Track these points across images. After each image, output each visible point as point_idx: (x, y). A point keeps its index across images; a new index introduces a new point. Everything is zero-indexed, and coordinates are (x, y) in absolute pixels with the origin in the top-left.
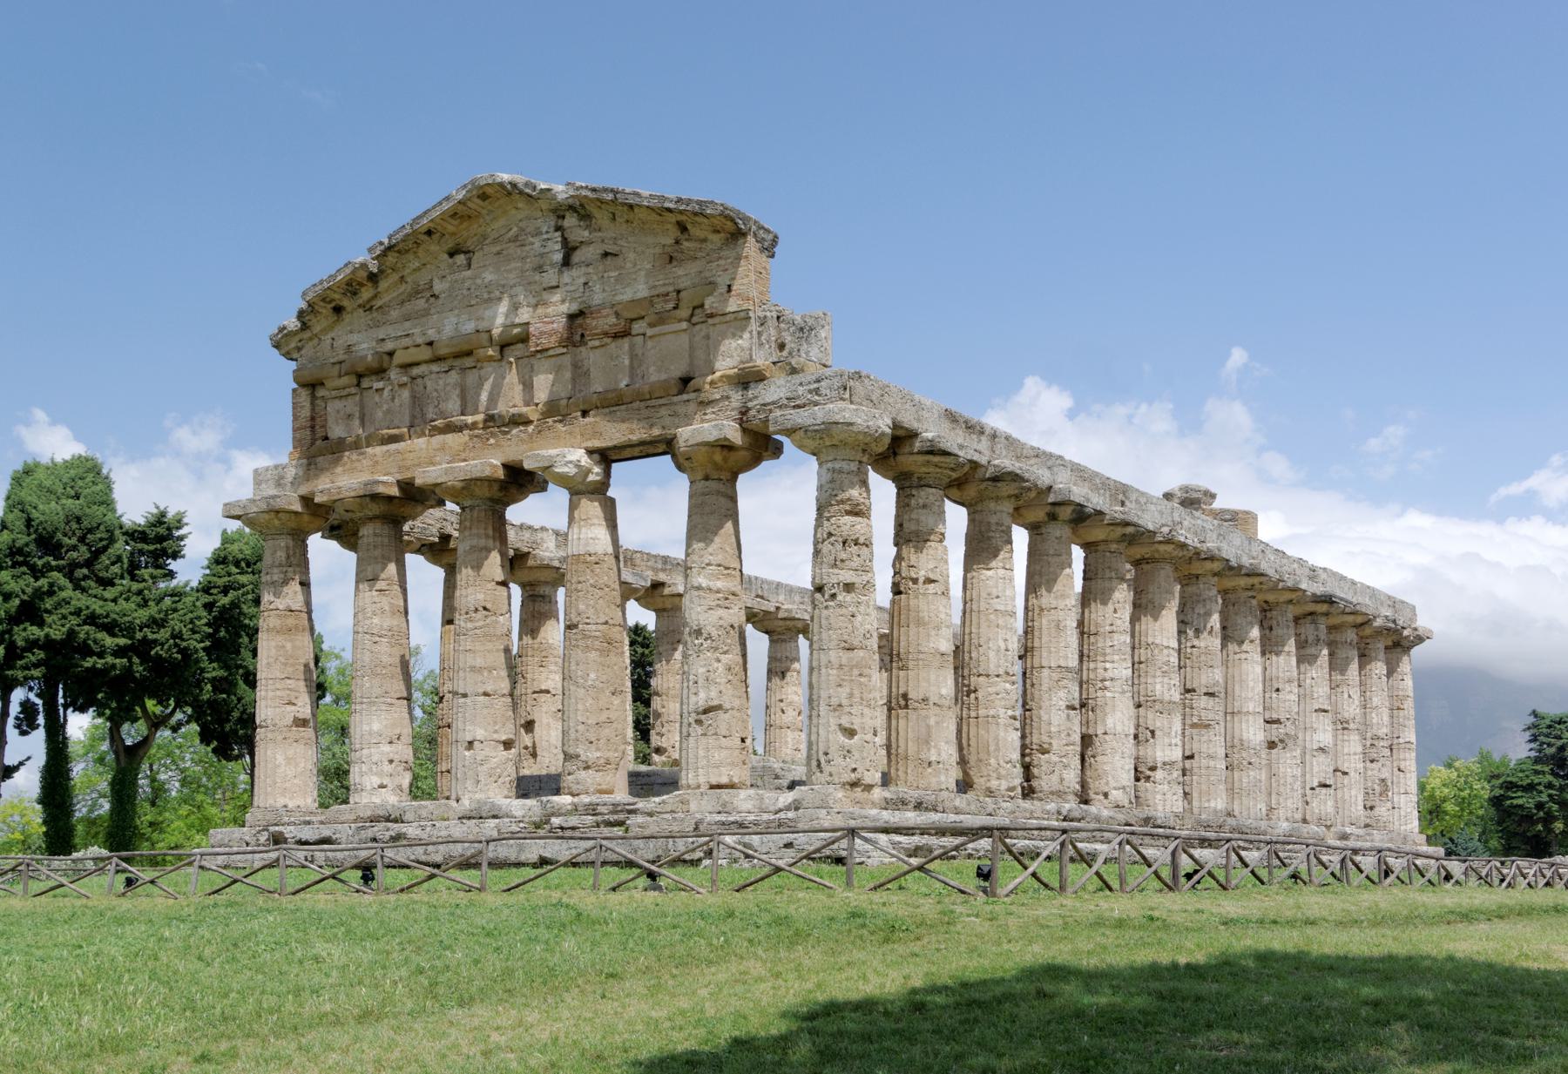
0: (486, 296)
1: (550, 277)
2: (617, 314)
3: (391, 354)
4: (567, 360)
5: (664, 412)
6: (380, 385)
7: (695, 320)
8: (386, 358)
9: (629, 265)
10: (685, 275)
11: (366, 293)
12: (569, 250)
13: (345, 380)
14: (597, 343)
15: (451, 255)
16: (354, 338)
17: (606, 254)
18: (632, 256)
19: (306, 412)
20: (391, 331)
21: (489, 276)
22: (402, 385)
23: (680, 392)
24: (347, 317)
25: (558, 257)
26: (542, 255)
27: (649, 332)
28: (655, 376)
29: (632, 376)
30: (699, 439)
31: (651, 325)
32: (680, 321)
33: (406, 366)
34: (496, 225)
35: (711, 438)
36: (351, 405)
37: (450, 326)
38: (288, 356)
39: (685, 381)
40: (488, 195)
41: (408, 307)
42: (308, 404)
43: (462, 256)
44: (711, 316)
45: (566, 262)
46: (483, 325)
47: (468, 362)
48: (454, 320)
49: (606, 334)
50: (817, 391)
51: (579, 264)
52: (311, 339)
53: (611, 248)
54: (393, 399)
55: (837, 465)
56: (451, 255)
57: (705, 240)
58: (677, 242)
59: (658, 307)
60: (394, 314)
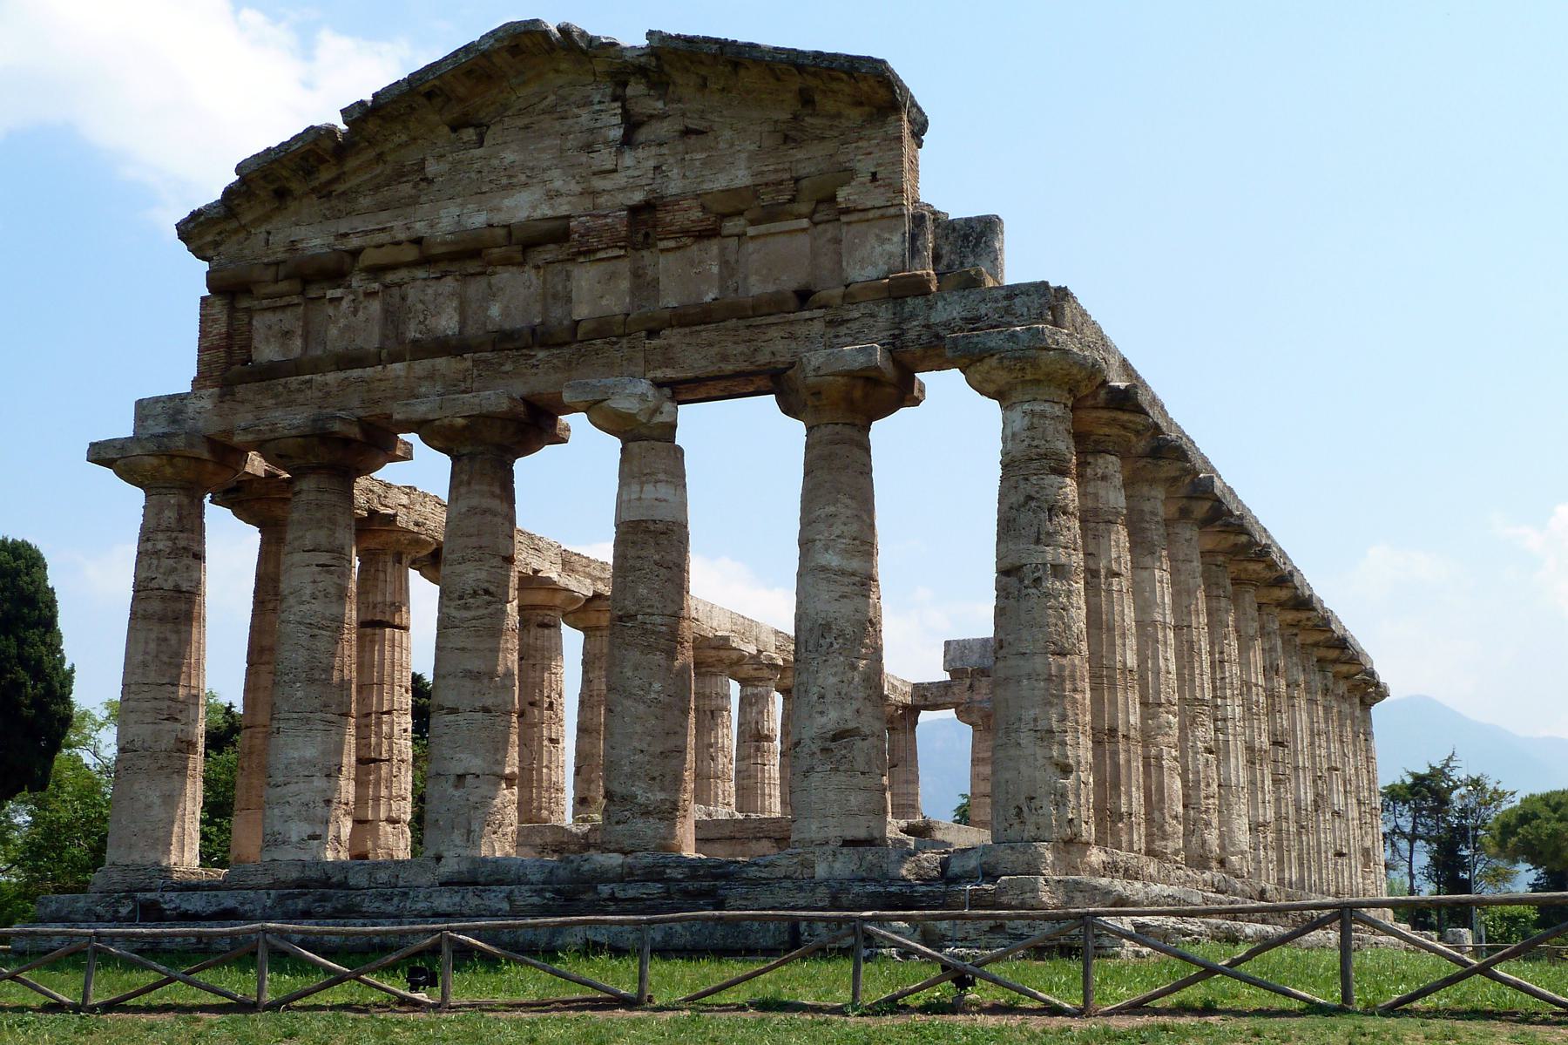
0: (504, 181)
1: (605, 158)
2: (704, 208)
3: (355, 253)
5: (773, 333)
6: (338, 293)
7: (817, 217)
8: (348, 259)
9: (722, 145)
10: (809, 160)
11: (325, 175)
12: (632, 125)
13: (283, 286)
14: (672, 244)
15: (455, 128)
16: (299, 233)
17: (687, 132)
18: (727, 134)
19: (221, 328)
20: (359, 223)
21: (510, 156)
22: (370, 295)
23: (801, 309)
24: (293, 205)
25: (617, 133)
26: (591, 131)
27: (751, 231)
28: (757, 287)
29: (723, 288)
30: (839, 367)
31: (753, 223)
32: (799, 217)
33: (376, 271)
34: (523, 92)
35: (856, 366)
36: (289, 320)
37: (447, 219)
38: (199, 253)
39: (804, 297)
40: (523, 51)
41: (386, 193)
42: (224, 318)
43: (471, 130)
44: (847, 211)
45: (627, 141)
46: (498, 218)
47: (472, 266)
48: (455, 211)
49: (686, 232)
50: (1008, 310)
51: (647, 144)
52: (236, 231)
53: (693, 124)
54: (355, 313)
55: (1038, 408)
56: (455, 128)
57: (839, 115)
58: (795, 118)
59: (767, 199)
60: (364, 202)
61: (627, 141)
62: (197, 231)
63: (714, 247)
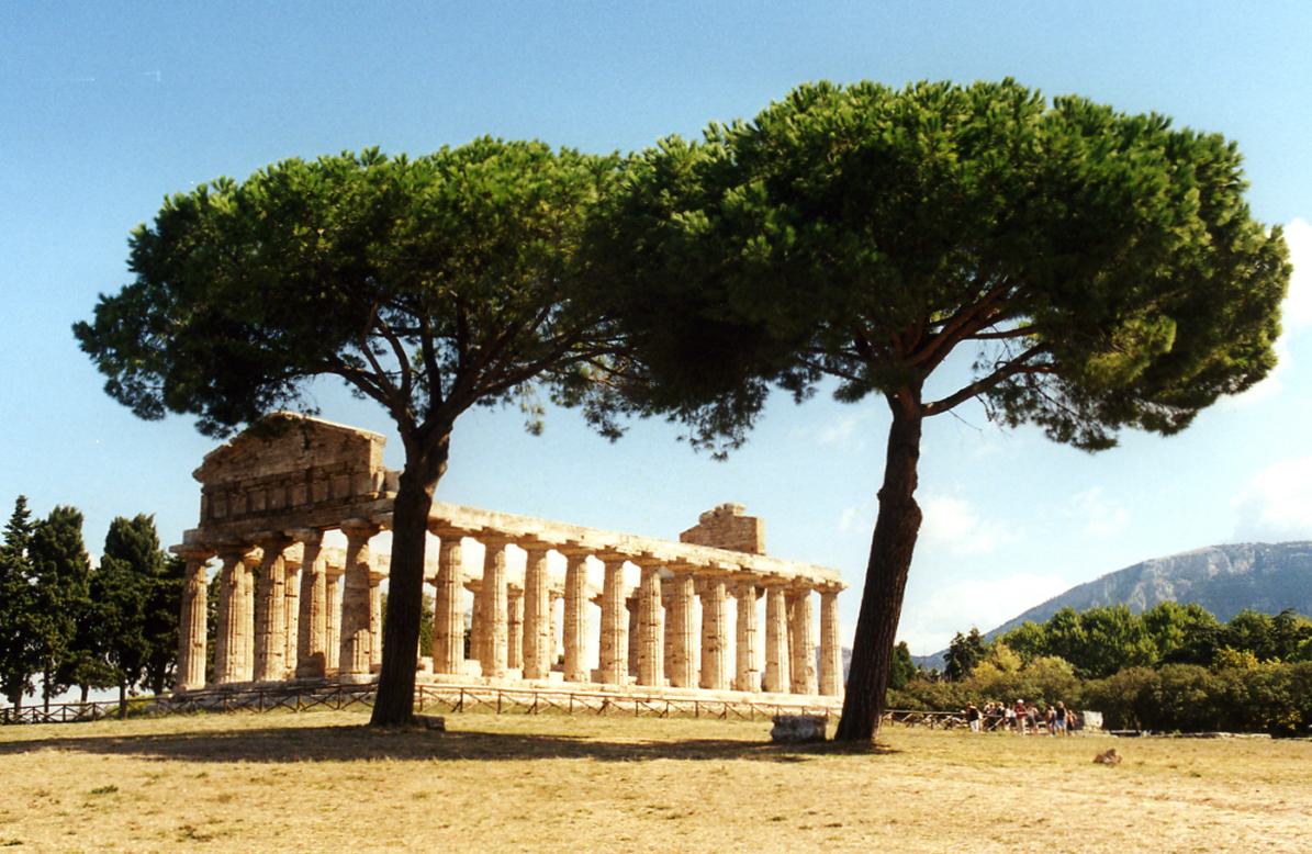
4: (305, 489)
10: (348, 455)
13: (222, 493)
33: (246, 488)
37: (264, 471)
38: (200, 481)
39: (346, 500)
45: (307, 448)
60: (242, 465)
61: (307, 448)
62: (198, 475)
63: (326, 483)
